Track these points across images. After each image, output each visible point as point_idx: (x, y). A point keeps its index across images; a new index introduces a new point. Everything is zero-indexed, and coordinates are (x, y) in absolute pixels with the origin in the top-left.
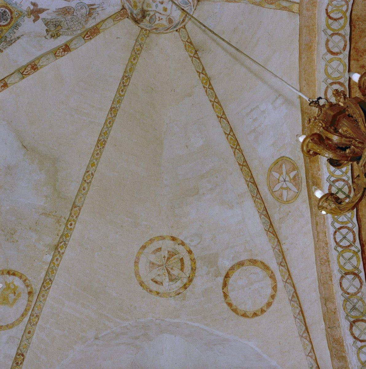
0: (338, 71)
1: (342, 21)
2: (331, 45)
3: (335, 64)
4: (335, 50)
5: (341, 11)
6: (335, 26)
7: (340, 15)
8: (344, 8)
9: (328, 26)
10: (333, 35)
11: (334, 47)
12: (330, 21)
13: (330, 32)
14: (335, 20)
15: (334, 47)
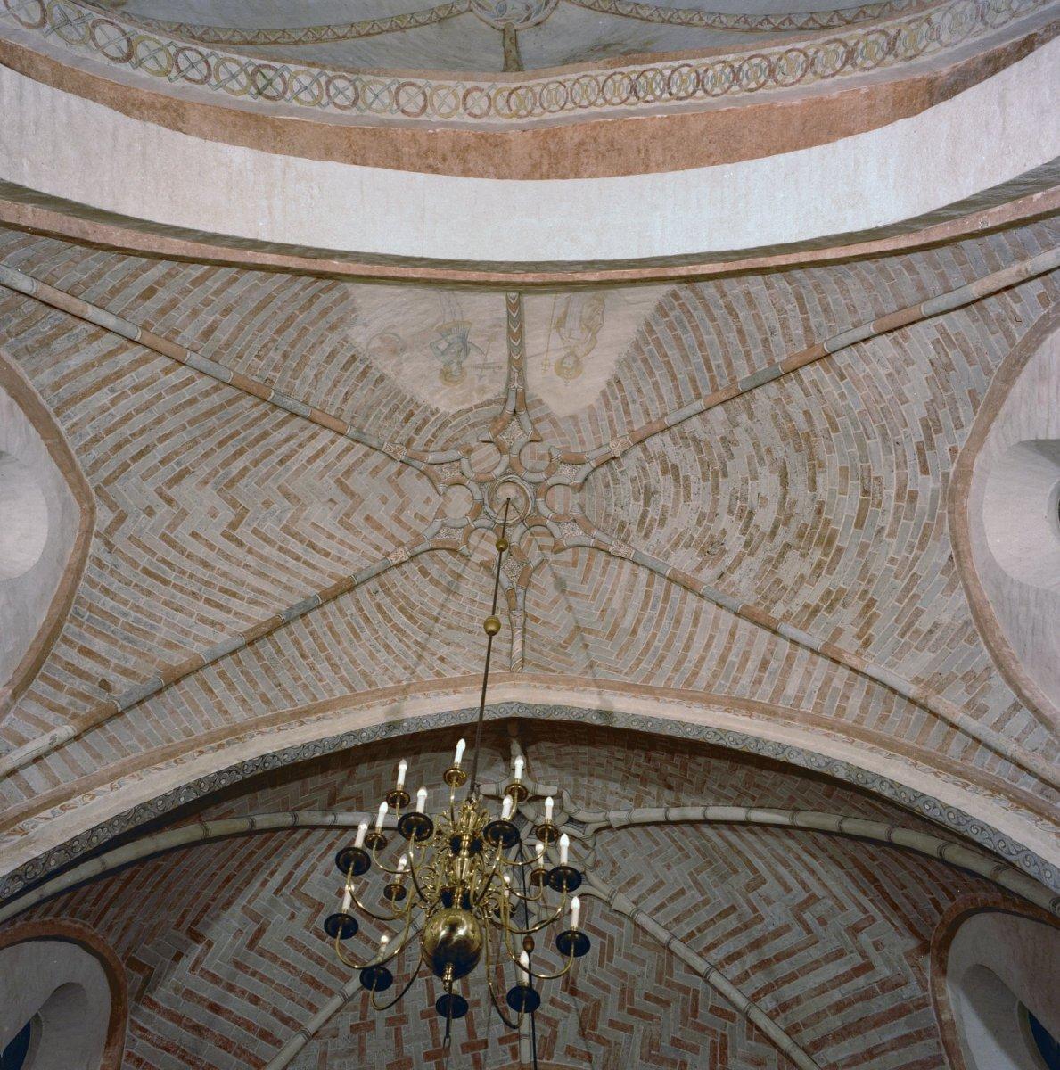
0: (442, 105)
1: (506, 111)
2: (476, 94)
3: (451, 101)
4: (469, 102)
5: (518, 110)
6: (500, 102)
7: (514, 108)
8: (523, 113)
9: (500, 91)
10: (489, 97)
11: (473, 99)
12: (506, 94)
13: (492, 93)
14: (508, 101)
15: (473, 99)
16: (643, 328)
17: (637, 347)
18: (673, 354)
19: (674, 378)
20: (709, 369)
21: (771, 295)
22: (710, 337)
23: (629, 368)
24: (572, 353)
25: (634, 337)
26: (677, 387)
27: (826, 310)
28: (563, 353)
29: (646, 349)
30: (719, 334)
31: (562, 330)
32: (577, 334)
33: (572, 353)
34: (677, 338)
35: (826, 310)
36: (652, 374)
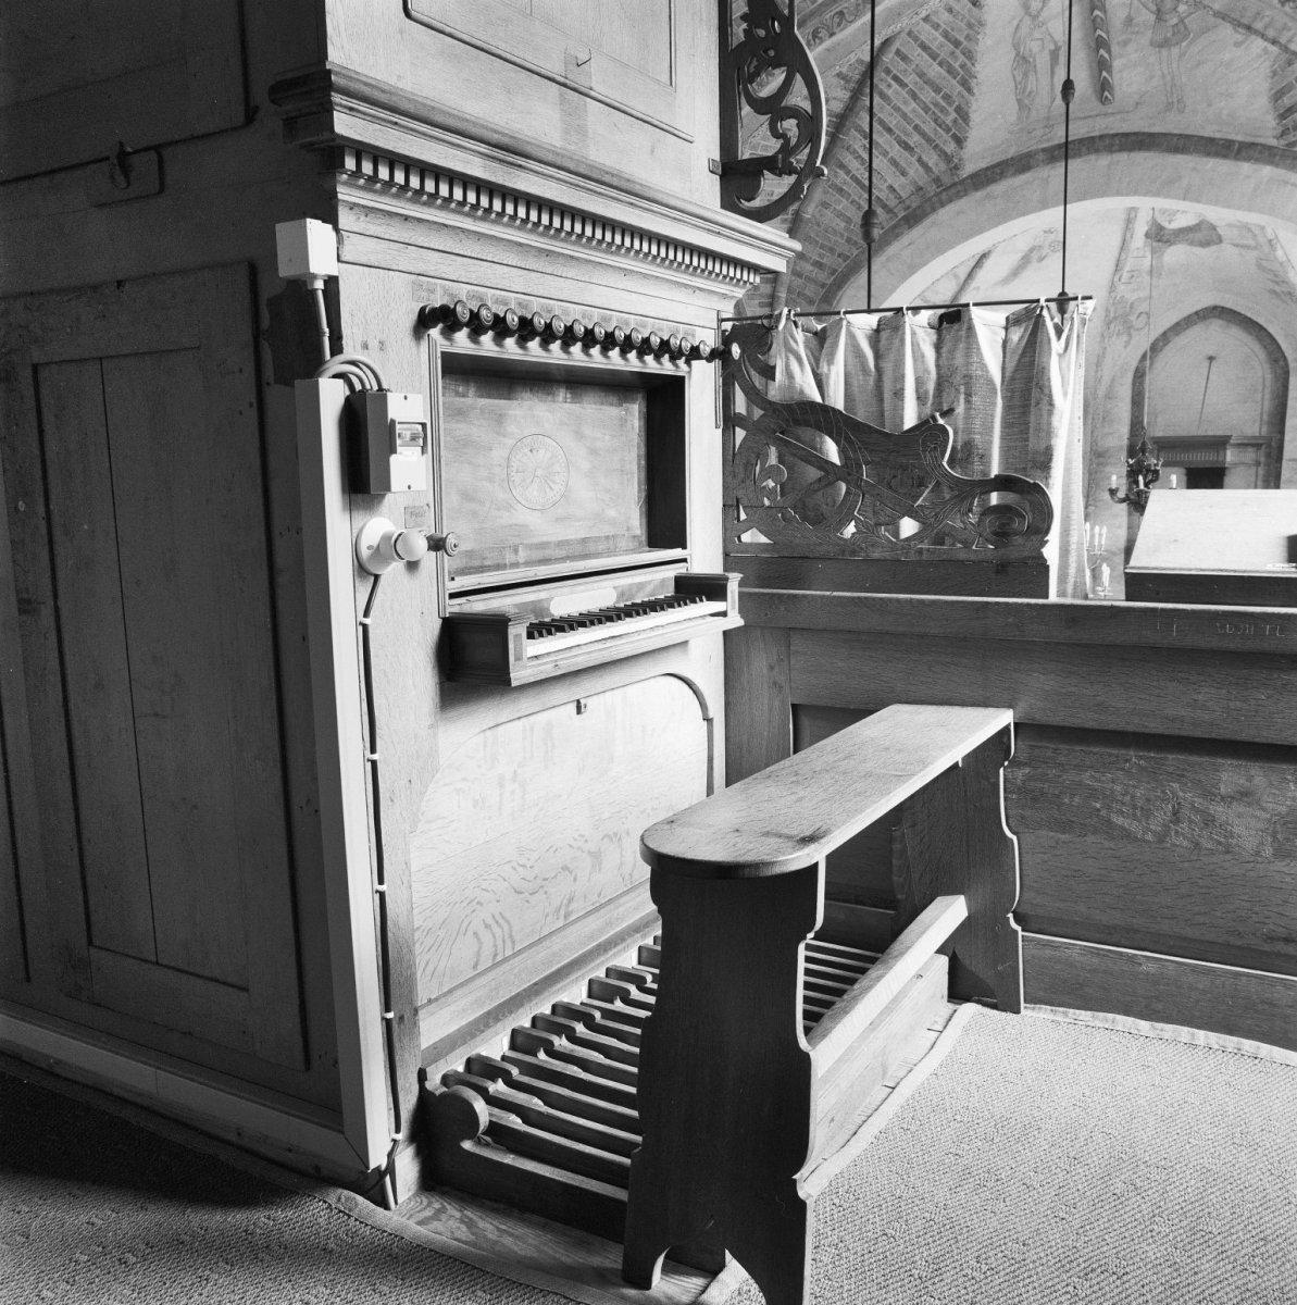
16: (973, 83)
17: (969, 55)
18: (935, 71)
19: (924, 47)
20: (896, 78)
21: (885, 181)
22: (911, 107)
23: (970, 26)
24: (1035, 18)
25: (978, 67)
26: (916, 39)
27: (840, 191)
28: (1045, 14)
29: (962, 58)
30: (904, 116)
31: (1052, 47)
32: (1035, 46)
33: (1035, 18)
34: (937, 90)
35: (840, 191)
36: (946, 35)
